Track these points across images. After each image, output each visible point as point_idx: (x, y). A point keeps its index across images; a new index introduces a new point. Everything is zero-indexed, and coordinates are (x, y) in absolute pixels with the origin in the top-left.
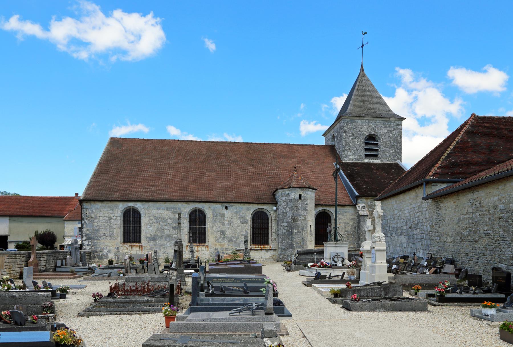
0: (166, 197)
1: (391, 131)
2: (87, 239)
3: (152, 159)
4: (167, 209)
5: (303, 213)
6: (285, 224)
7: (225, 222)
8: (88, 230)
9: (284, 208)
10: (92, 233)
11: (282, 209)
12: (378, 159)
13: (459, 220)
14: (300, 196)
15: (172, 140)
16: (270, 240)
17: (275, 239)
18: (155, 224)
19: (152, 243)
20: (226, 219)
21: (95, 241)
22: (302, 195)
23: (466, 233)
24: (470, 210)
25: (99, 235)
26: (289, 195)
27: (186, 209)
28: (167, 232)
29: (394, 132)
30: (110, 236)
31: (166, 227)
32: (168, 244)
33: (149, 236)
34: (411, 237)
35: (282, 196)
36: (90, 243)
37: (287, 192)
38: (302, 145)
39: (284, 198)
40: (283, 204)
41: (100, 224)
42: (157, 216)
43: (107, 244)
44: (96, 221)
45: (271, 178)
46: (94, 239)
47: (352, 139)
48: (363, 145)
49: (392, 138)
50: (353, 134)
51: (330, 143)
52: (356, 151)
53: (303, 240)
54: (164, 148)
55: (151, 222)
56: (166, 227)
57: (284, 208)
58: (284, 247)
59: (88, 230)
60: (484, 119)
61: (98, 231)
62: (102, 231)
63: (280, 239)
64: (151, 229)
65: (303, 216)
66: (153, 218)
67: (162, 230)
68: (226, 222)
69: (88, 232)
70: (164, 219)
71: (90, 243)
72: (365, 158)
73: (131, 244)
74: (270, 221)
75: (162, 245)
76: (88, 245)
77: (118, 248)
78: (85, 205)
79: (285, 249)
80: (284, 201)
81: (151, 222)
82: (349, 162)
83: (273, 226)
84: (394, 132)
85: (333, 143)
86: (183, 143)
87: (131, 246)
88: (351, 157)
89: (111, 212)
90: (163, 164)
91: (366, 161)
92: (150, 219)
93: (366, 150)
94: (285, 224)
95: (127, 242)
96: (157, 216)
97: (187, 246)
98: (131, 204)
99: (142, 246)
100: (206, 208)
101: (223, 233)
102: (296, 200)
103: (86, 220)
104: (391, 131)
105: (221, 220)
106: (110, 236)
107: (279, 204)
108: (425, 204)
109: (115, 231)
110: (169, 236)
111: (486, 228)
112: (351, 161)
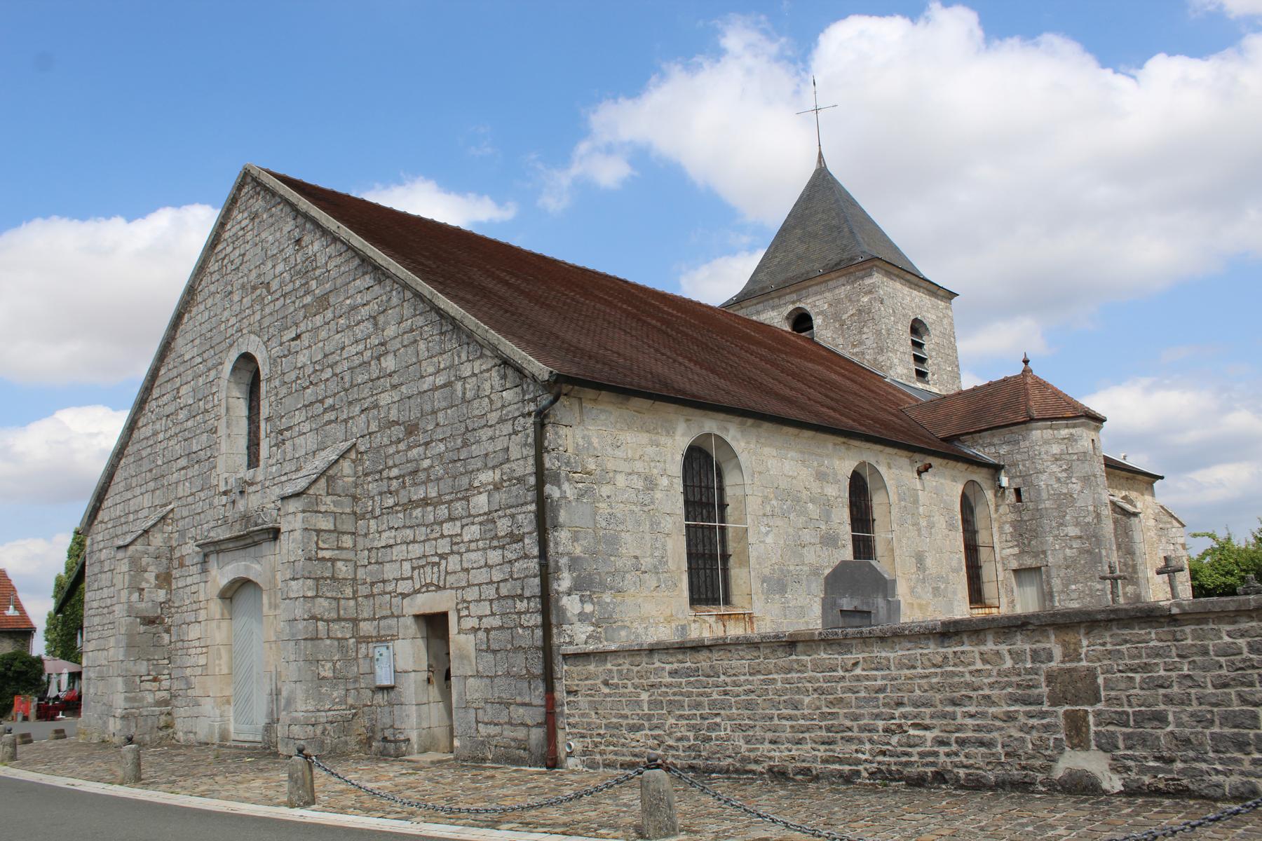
2: (576, 587)
6: (1072, 531)
8: (575, 539)
9: (1058, 480)
11: (1053, 482)
12: (927, 382)
18: (779, 522)
20: (921, 509)
21: (607, 598)
25: (619, 564)
26: (1071, 439)
30: (655, 570)
31: (807, 536)
33: (767, 572)
36: (588, 608)
39: (1056, 449)
40: (1054, 468)
41: (619, 510)
43: (649, 609)
44: (605, 490)
46: (604, 587)
57: (1058, 480)
61: (613, 542)
62: (629, 545)
64: (769, 540)
68: (923, 523)
69: (578, 551)
71: (588, 608)
73: (723, 610)
76: (583, 617)
77: (683, 627)
78: (564, 410)
80: (1057, 459)
87: (721, 617)
89: (651, 450)
92: (766, 500)
94: (1072, 531)
95: (715, 601)
98: (711, 425)
101: (920, 559)
103: (566, 486)
106: (655, 570)
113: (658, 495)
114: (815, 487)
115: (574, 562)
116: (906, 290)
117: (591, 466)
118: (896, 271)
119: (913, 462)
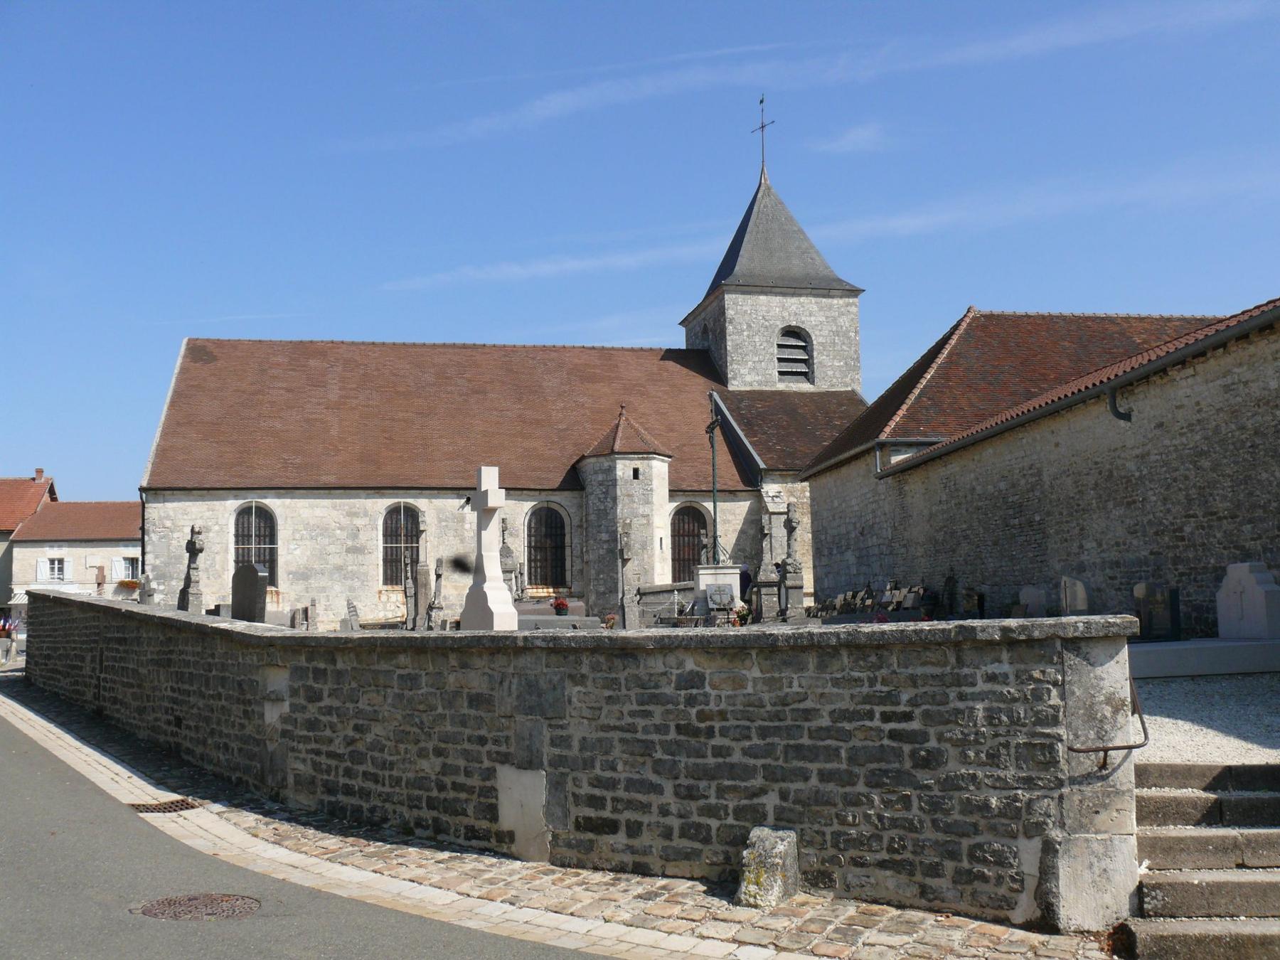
0: (331, 479)
1: (835, 319)
3: (288, 390)
4: (334, 507)
5: (642, 510)
6: (604, 536)
7: (466, 534)
8: (156, 557)
10: (167, 564)
13: (931, 515)
14: (636, 472)
15: (328, 343)
16: (568, 575)
17: (581, 571)
18: (308, 543)
19: (300, 586)
22: (641, 470)
23: (940, 537)
24: (944, 498)
27: (379, 506)
28: (336, 560)
29: (841, 321)
31: (332, 549)
32: (337, 588)
34: (864, 552)
35: (596, 473)
37: (606, 464)
38: (632, 350)
39: (600, 477)
42: (312, 522)
44: (176, 535)
45: (567, 429)
46: (172, 579)
47: (748, 336)
48: (775, 350)
49: (837, 333)
50: (749, 326)
51: (699, 345)
52: (758, 366)
53: (646, 572)
54: (312, 363)
55: (298, 536)
56: (332, 549)
58: (602, 589)
59: (156, 557)
60: (990, 317)
63: (593, 572)
64: (298, 552)
65: (643, 516)
66: (301, 527)
67: (323, 555)
69: (158, 562)
70: (327, 529)
72: (780, 380)
74: (567, 529)
75: (323, 589)
79: (604, 593)
81: (298, 536)
82: (743, 389)
83: (576, 541)
84: (841, 321)
85: (706, 344)
86: (353, 348)
88: (748, 378)
90: (314, 400)
91: (781, 386)
92: (295, 531)
93: (780, 360)
96: (312, 522)
97: (380, 592)
99: (277, 593)
100: (422, 503)
102: (626, 481)
103: (152, 535)
104: (835, 319)
105: (456, 530)
107: (589, 489)
108: (882, 486)
109: (218, 558)
110: (339, 568)
111: (964, 526)
112: (748, 389)
113: (211, 534)
114: (345, 521)
115: (154, 568)
116: (776, 300)
117: (168, 523)
118: (759, 289)
119: (460, 497)
